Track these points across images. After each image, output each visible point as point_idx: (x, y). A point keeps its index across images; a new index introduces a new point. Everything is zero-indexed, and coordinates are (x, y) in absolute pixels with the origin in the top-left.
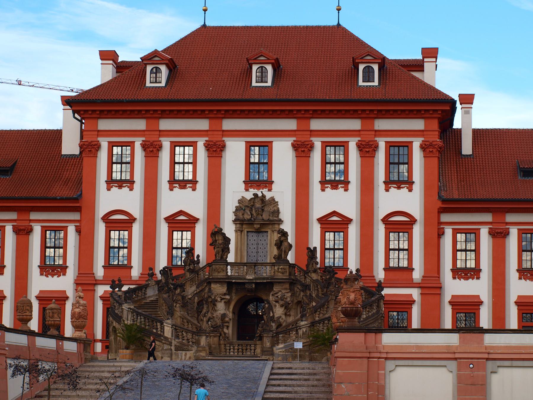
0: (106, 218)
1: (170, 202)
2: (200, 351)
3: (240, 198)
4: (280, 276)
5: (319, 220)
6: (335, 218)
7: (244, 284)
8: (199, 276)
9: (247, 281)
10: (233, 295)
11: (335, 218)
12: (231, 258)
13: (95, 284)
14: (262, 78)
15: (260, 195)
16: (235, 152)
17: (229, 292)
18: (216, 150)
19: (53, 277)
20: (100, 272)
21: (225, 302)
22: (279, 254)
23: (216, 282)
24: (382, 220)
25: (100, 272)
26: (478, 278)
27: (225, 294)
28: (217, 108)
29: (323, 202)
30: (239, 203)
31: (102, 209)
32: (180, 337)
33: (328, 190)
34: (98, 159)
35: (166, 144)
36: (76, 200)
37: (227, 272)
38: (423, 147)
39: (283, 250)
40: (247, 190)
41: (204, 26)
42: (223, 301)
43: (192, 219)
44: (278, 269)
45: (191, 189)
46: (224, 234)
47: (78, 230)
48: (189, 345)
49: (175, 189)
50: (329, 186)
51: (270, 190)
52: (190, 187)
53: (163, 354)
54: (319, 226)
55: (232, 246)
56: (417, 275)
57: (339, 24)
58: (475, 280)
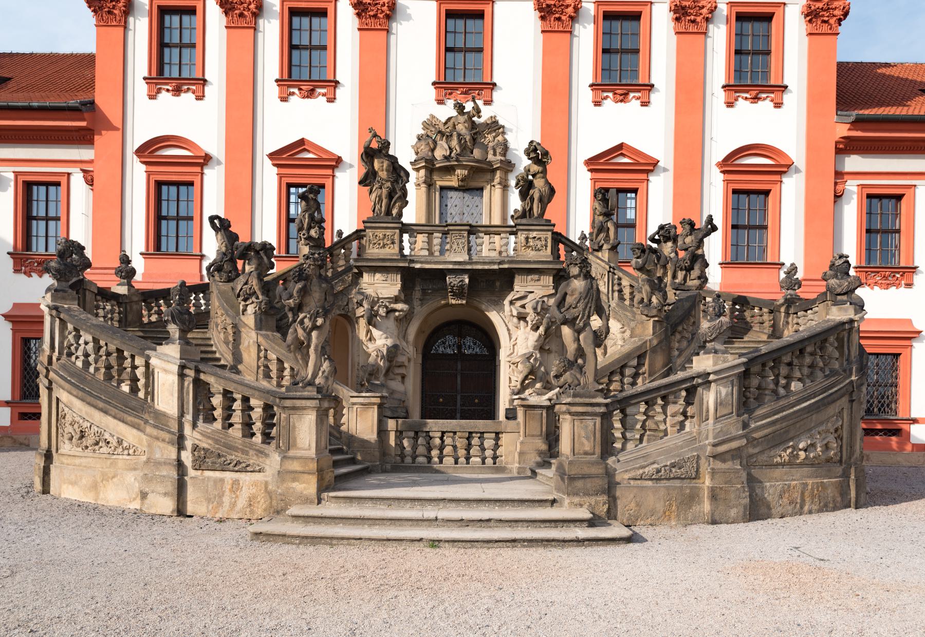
2: (295, 475)
3: (426, 117)
4: (531, 255)
7: (442, 273)
8: (335, 259)
9: (451, 267)
10: (416, 303)
12: (410, 215)
15: (469, 106)
17: (407, 293)
19: (41, 277)
21: (397, 319)
22: (524, 210)
23: (374, 270)
24: (719, 165)
26: (909, 285)
27: (396, 300)
29: (600, 125)
30: (425, 128)
32: (218, 413)
33: (609, 104)
37: (402, 249)
39: (536, 196)
40: (440, 102)
42: (392, 315)
43: (324, 157)
44: (527, 239)
45: (324, 99)
46: (394, 160)
48: (251, 446)
49: (292, 98)
50: (610, 95)
51: (488, 103)
52: (324, 95)
53: (146, 478)
55: (414, 191)
58: (902, 289)
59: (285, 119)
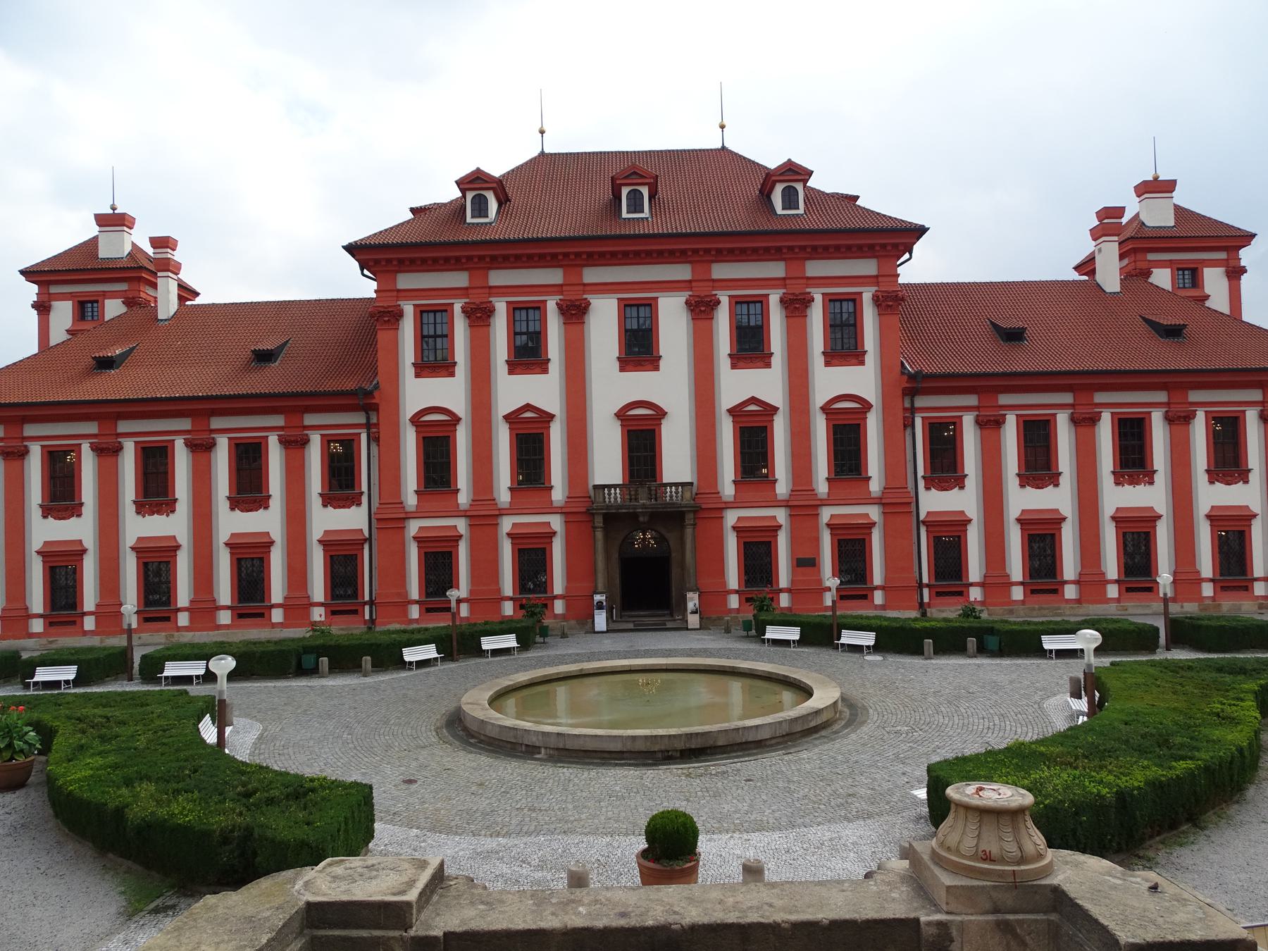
0: (416, 420)
1: (514, 392)
5: (731, 411)
6: (753, 408)
11: (753, 408)
13: (404, 519)
14: (636, 205)
16: (604, 320)
18: (575, 313)
20: (411, 500)
24: (822, 408)
25: (411, 500)
28: (570, 253)
31: (410, 406)
34: (400, 332)
35: (501, 306)
36: (369, 394)
38: (877, 300)
41: (542, 153)
47: (374, 439)
54: (731, 419)
56: (875, 486)
57: (723, 147)
59: (514, 392)
